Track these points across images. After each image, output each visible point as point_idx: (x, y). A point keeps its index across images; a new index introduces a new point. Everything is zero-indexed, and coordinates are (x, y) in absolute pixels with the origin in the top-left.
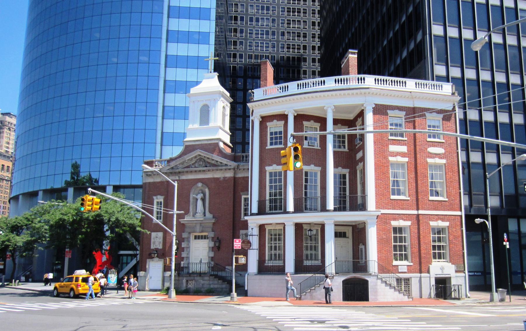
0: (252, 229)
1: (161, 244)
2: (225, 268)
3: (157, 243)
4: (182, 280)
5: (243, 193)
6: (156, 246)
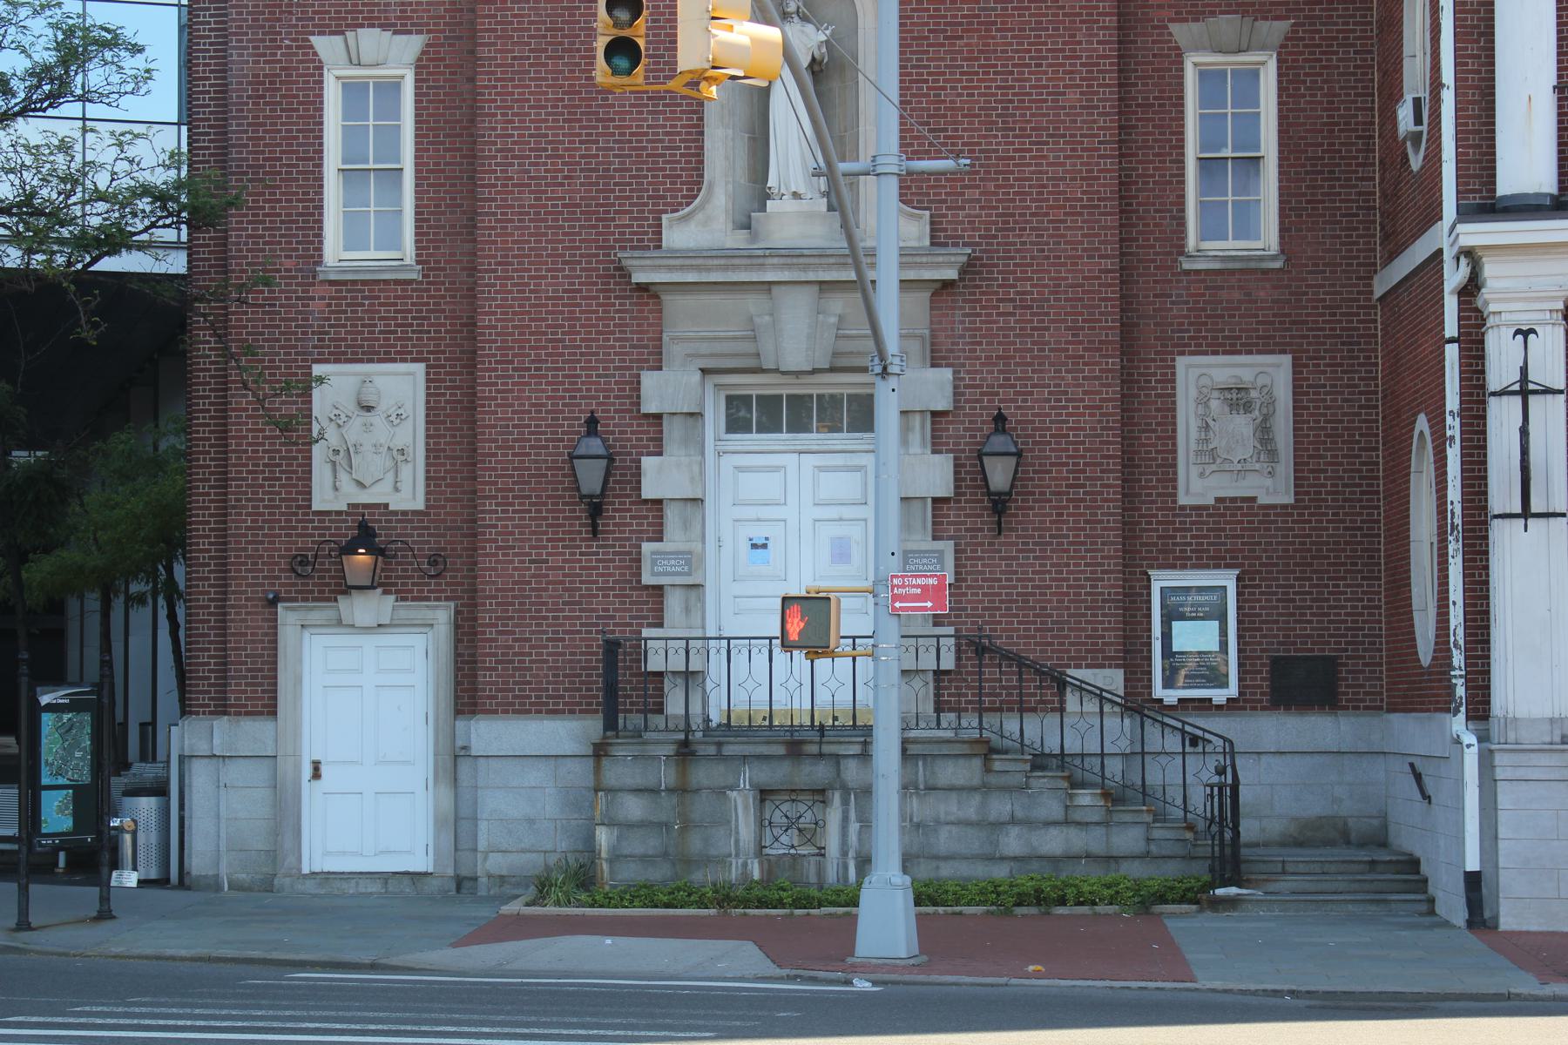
0: (1526, 333)
1: (406, 472)
2: (1062, 685)
3: (371, 464)
4: (721, 792)
5: (1195, 27)
6: (361, 485)
